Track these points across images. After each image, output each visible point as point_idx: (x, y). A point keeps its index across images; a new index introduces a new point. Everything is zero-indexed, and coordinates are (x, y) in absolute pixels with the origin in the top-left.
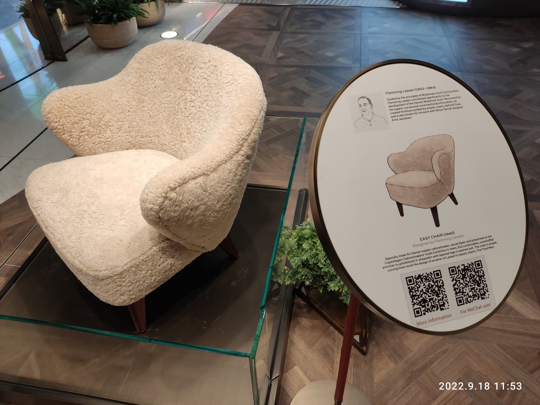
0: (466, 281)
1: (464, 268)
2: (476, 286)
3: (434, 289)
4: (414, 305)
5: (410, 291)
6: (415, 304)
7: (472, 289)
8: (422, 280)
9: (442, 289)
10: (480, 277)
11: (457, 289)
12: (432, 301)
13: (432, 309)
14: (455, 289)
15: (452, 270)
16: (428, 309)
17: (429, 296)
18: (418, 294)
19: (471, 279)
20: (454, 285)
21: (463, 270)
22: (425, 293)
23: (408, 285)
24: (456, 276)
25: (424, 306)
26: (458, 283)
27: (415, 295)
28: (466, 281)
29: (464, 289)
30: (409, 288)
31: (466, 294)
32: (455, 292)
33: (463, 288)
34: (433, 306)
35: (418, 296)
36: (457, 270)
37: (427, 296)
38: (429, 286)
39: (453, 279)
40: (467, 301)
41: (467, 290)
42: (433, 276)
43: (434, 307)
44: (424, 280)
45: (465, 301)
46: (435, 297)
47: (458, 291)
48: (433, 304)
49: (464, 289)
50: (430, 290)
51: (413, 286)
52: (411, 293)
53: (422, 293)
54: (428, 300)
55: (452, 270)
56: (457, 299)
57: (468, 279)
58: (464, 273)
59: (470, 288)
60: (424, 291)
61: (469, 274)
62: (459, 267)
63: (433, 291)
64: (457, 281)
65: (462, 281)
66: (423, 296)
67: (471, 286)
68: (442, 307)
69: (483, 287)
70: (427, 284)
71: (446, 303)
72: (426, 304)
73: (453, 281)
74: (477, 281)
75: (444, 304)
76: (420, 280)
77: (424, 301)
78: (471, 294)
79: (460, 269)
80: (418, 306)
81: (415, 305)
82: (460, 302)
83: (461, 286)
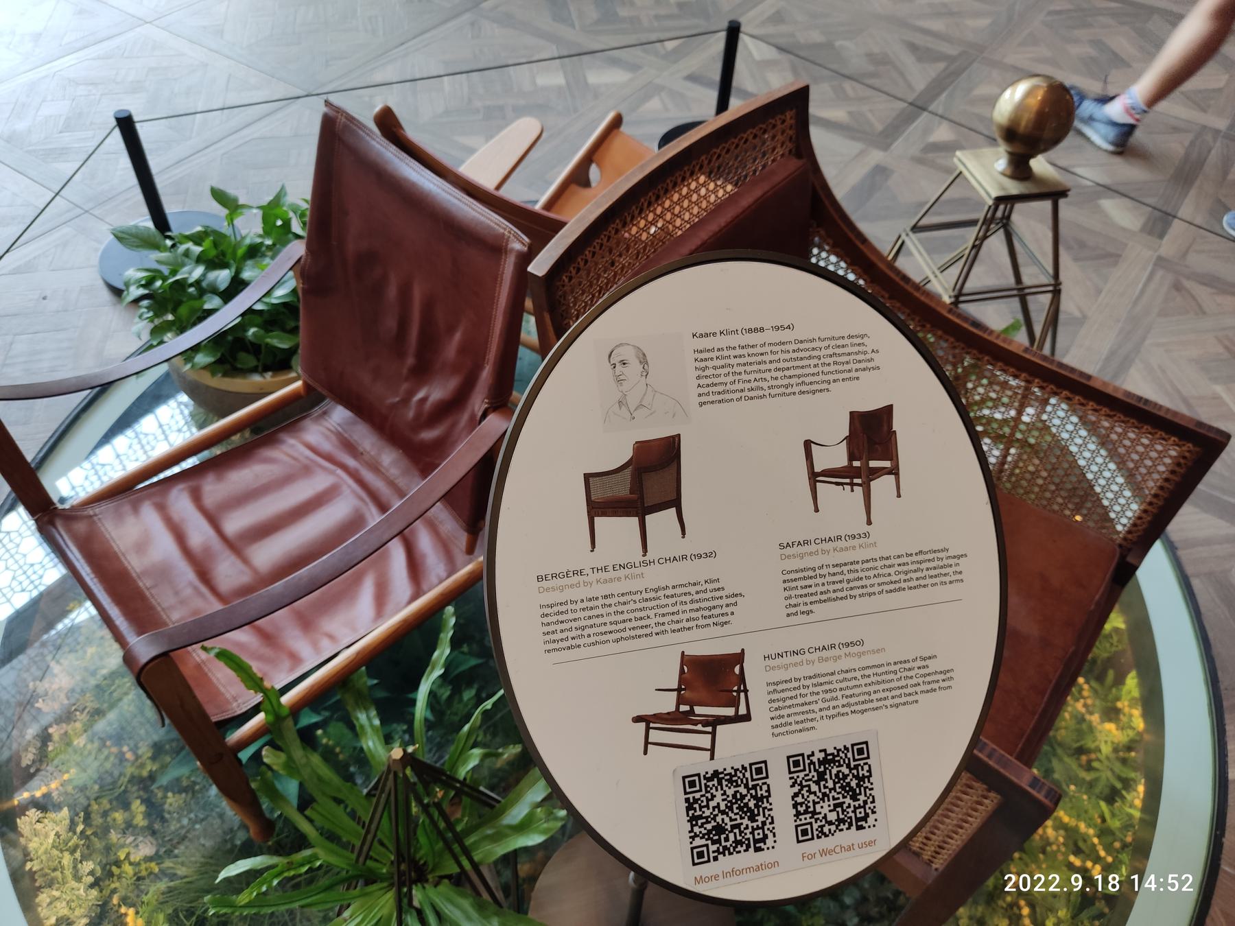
0: (825, 787)
1: (825, 758)
2: (848, 800)
3: (848, 784)
4: (693, 838)
5: (688, 809)
6: (696, 836)
7: (836, 806)
8: (720, 783)
9: (765, 805)
10: (861, 779)
11: (801, 804)
12: (737, 831)
13: (734, 848)
14: (795, 806)
15: (794, 762)
16: (725, 848)
17: (731, 820)
18: (707, 813)
19: (839, 782)
20: (796, 795)
21: (821, 763)
22: (723, 812)
23: (686, 793)
24: (802, 775)
25: (719, 842)
26: (804, 792)
27: (700, 817)
28: (825, 787)
29: (818, 807)
30: (687, 800)
31: (820, 817)
32: (794, 812)
33: (815, 803)
34: (738, 843)
35: (706, 818)
36: (807, 762)
37: (727, 820)
38: (734, 796)
39: (796, 782)
40: (822, 832)
41: (824, 808)
42: (850, 755)
43: (741, 843)
44: (724, 783)
45: (815, 833)
46: (746, 821)
47: (801, 809)
48: (739, 838)
49: (818, 807)
50: (735, 806)
51: (697, 795)
52: (691, 813)
53: (716, 812)
54: (728, 827)
55: (794, 762)
56: (797, 827)
57: (830, 784)
58: (822, 769)
59: (832, 802)
60: (723, 807)
61: (834, 771)
62: (813, 754)
63: (745, 809)
64: (802, 787)
65: (814, 788)
66: (719, 819)
67: (834, 799)
68: (758, 845)
69: (865, 802)
70: (730, 792)
71: (770, 835)
72: (723, 836)
73: (793, 786)
74: (851, 788)
75: (766, 836)
76: (715, 782)
77: (719, 829)
78: (832, 817)
79: (814, 759)
80: (703, 842)
81: (697, 839)
82: (803, 835)
83: (812, 797)
